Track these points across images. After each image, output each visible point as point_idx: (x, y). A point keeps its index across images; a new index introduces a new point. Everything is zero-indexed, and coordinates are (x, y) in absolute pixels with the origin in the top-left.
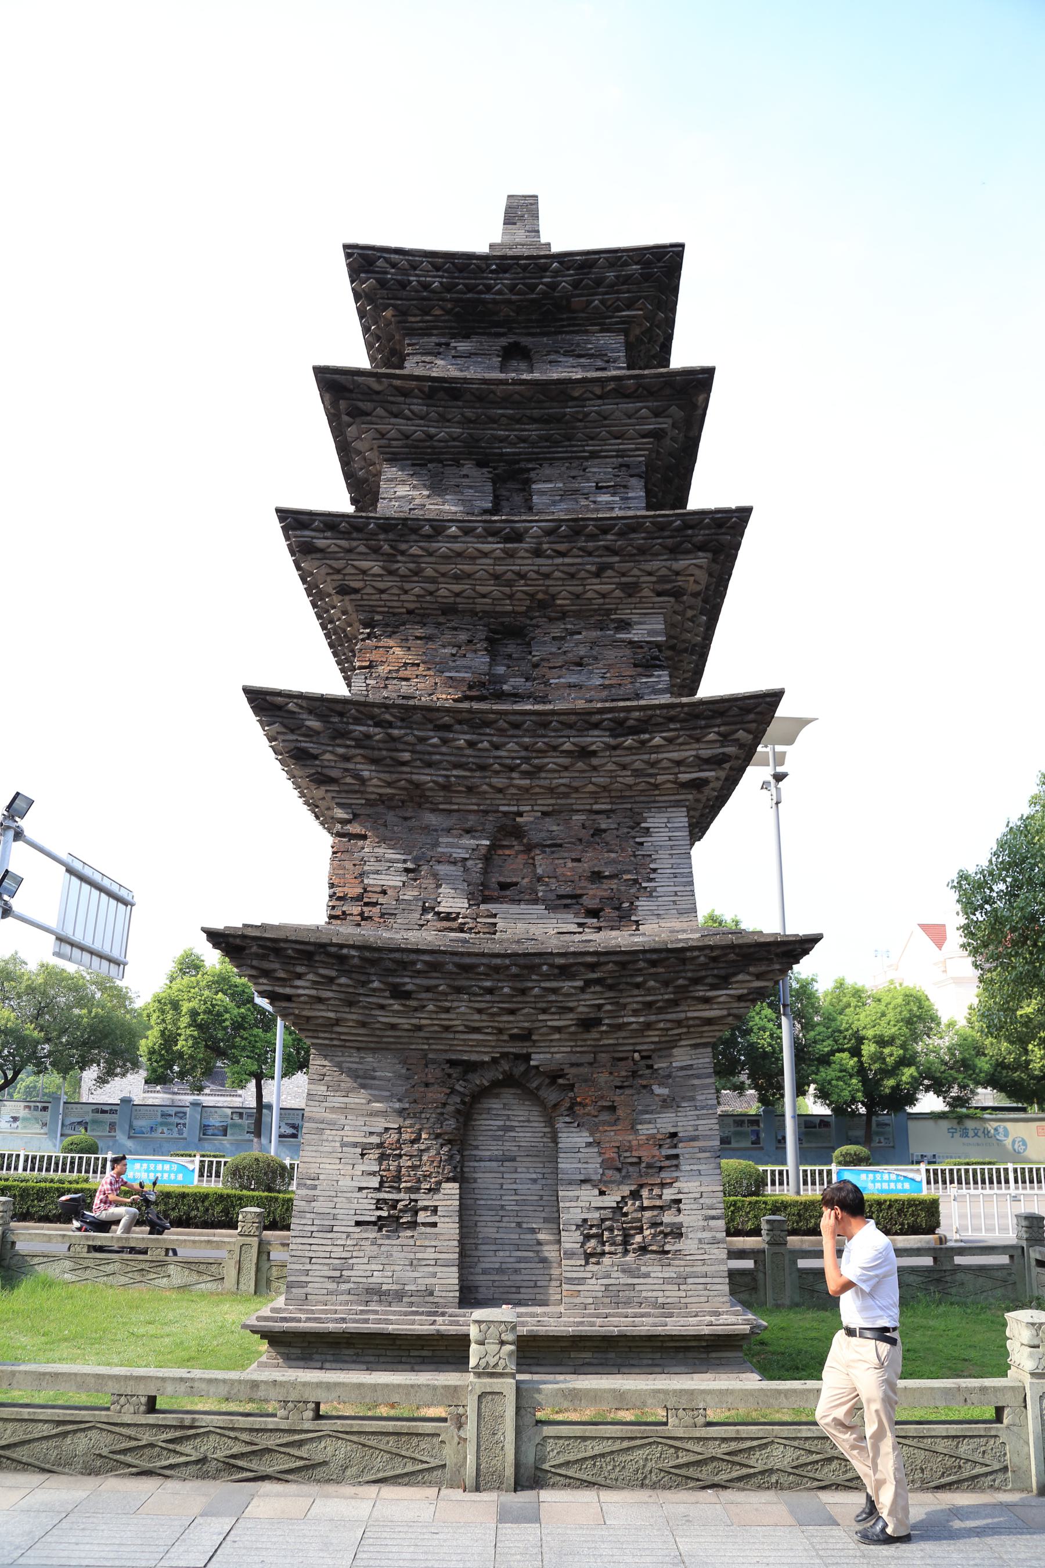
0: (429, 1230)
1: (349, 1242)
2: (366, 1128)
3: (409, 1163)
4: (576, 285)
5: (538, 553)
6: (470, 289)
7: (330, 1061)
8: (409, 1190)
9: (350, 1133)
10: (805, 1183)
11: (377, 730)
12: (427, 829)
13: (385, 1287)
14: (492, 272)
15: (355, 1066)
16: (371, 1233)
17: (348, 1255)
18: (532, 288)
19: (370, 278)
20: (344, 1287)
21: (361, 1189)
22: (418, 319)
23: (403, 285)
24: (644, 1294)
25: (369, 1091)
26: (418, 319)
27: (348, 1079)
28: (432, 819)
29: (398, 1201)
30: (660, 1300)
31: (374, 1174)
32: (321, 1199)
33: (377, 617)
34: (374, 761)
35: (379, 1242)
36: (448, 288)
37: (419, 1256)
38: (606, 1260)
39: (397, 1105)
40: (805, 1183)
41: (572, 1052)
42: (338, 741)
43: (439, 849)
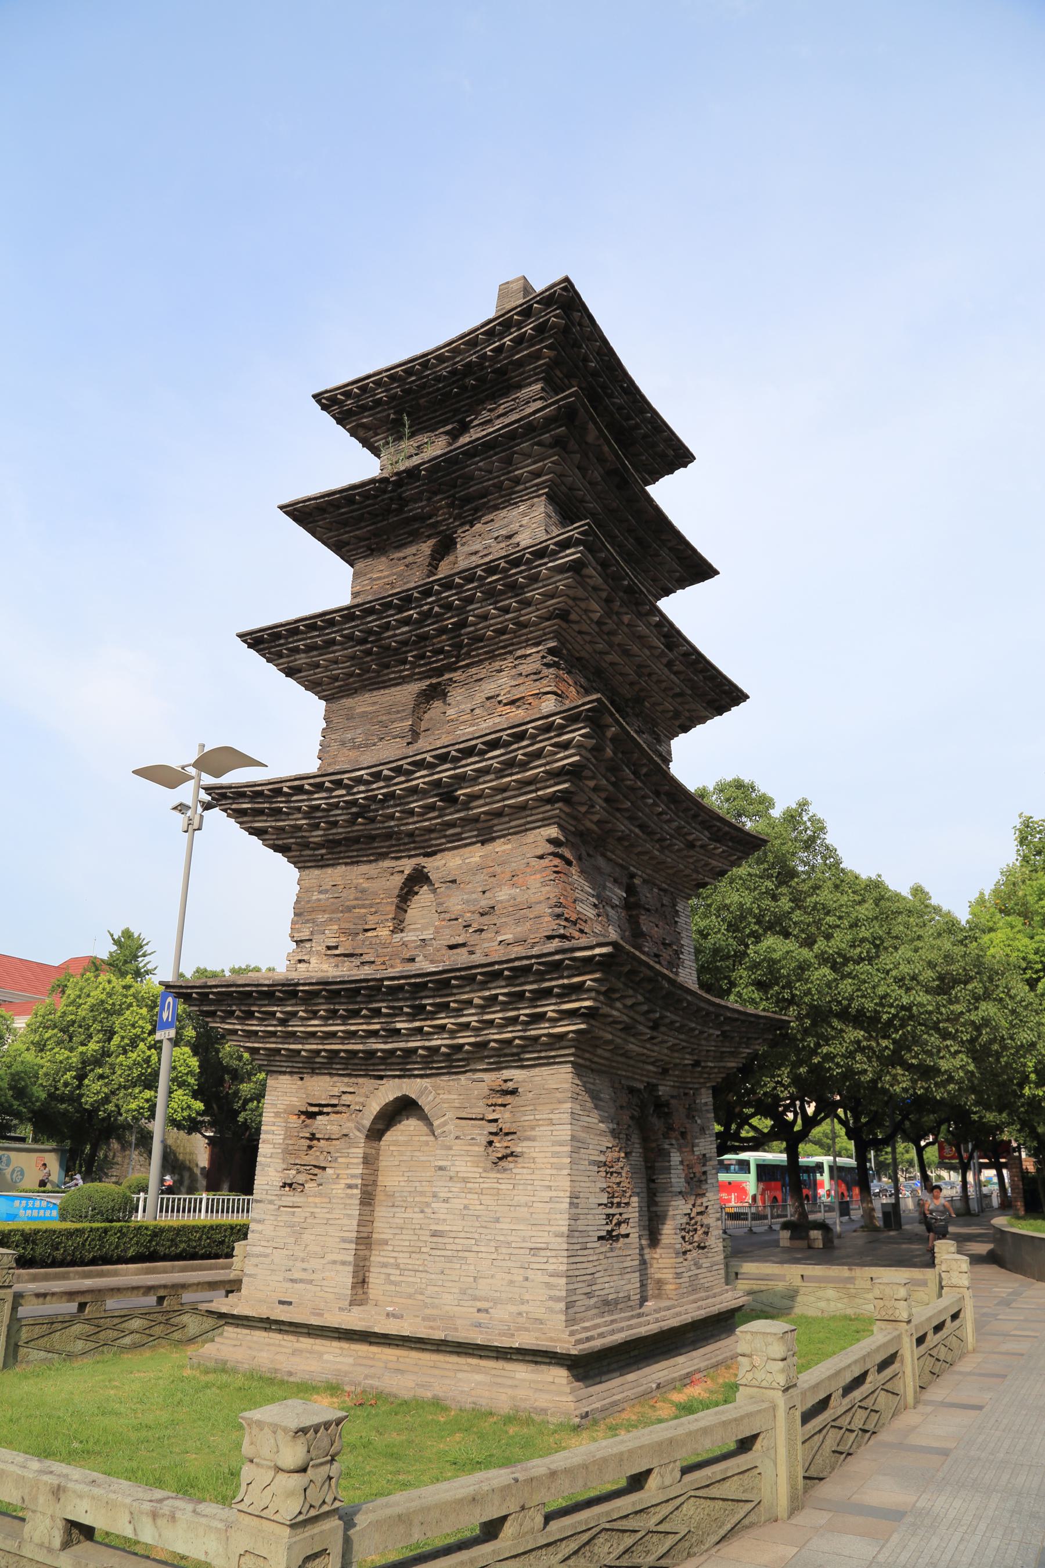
0: (626, 1240)
1: (595, 1258)
2: (598, 1147)
3: (618, 1180)
4: (645, 436)
5: (669, 665)
6: (604, 387)
7: (581, 1080)
8: (619, 1204)
9: (592, 1152)
10: (161, 1211)
11: (632, 777)
12: (598, 869)
13: (611, 1297)
14: (622, 387)
15: (592, 1087)
16: (605, 1246)
17: (593, 1270)
18: (629, 418)
19: (563, 319)
20: (593, 1301)
21: (600, 1205)
22: (561, 375)
23: (576, 345)
24: (702, 1281)
25: (601, 1113)
26: (561, 375)
27: (589, 1099)
28: (601, 862)
29: (614, 1215)
30: (706, 1285)
31: (603, 1190)
32: (582, 1217)
33: (564, 651)
34: (607, 800)
35: (608, 1255)
36: (595, 374)
37: (626, 1265)
38: (688, 1256)
39: (611, 1126)
40: (161, 1211)
41: (673, 1087)
42: (609, 774)
43: (608, 893)
